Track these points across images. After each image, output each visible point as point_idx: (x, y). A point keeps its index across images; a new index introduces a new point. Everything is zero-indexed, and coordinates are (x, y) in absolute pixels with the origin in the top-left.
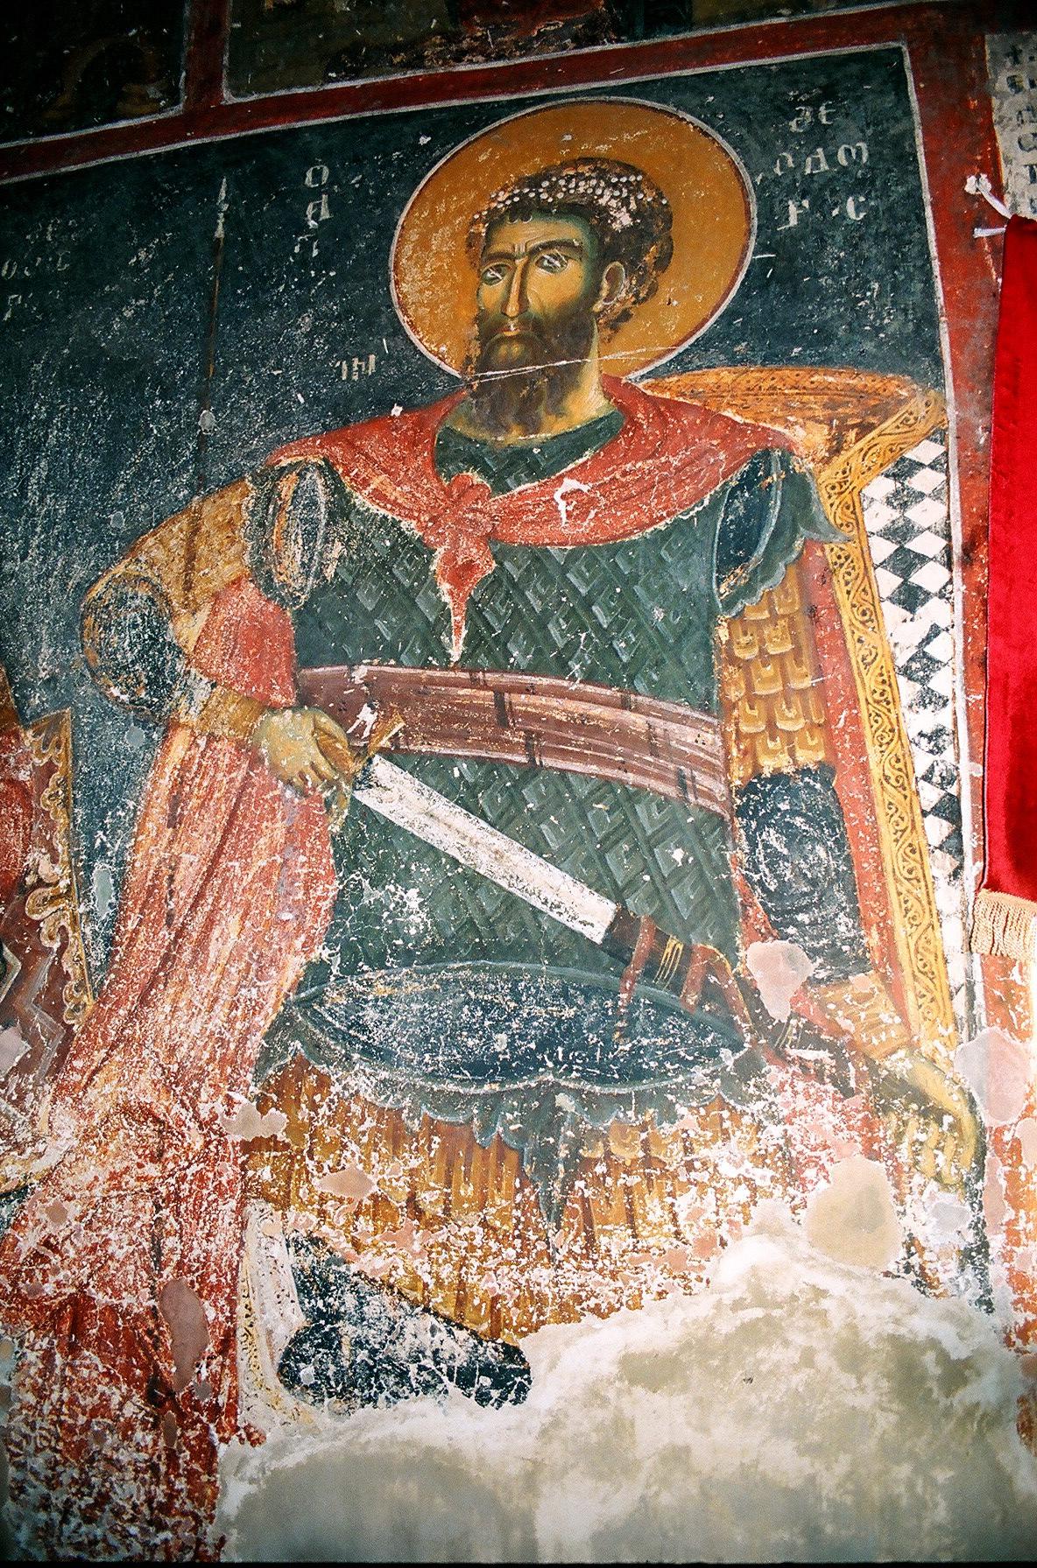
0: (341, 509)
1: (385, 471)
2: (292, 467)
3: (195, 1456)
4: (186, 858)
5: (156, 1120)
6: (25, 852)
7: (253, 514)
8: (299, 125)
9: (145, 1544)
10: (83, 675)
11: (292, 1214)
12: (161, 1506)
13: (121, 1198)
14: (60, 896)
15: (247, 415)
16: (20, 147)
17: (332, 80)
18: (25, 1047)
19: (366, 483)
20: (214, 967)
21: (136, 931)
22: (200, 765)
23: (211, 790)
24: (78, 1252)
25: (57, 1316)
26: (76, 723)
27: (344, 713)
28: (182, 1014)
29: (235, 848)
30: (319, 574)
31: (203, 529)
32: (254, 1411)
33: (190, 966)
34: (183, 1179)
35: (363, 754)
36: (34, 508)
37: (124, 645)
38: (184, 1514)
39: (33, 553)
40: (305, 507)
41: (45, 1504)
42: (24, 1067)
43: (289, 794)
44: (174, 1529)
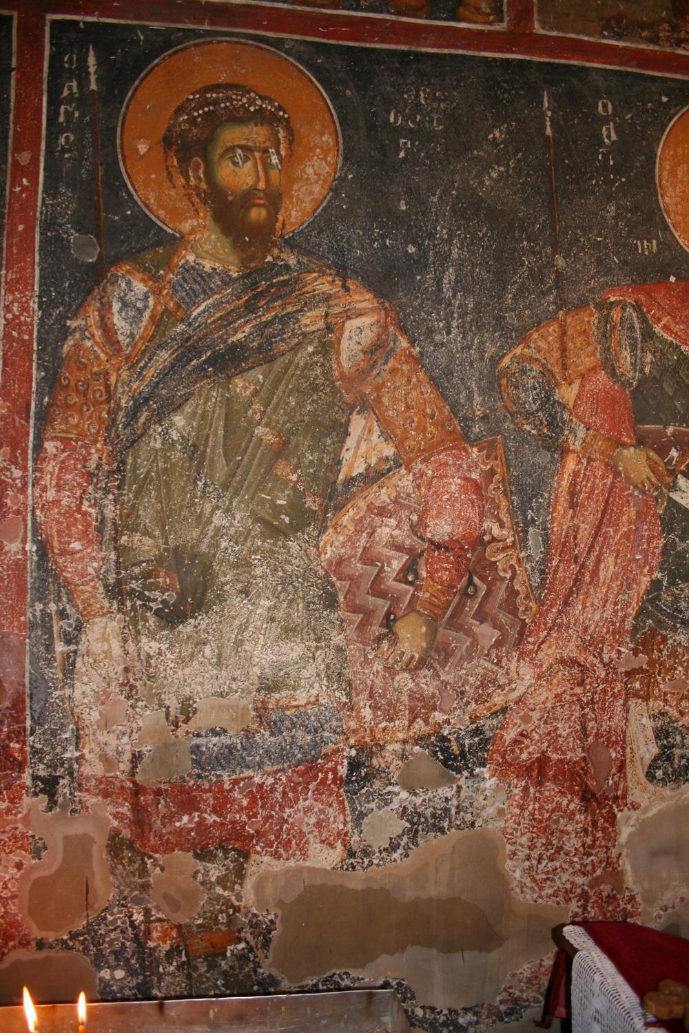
0: (648, 334)
1: (669, 314)
2: (617, 303)
3: (606, 821)
4: (583, 526)
5: (579, 665)
6: (481, 521)
7: (598, 328)
8: (588, 64)
9: (581, 864)
10: (505, 416)
11: (651, 703)
12: (589, 847)
13: (562, 706)
14: (508, 547)
15: (585, 264)
16: (386, 21)
17: (605, 37)
18: (497, 633)
19: (659, 320)
20: (604, 583)
21: (558, 566)
22: (585, 474)
23: (593, 489)
24: (540, 736)
25: (529, 769)
26: (505, 445)
27: (663, 451)
28: (589, 610)
29: (609, 520)
30: (642, 371)
31: (569, 333)
32: (635, 795)
33: (590, 584)
34: (595, 693)
35: (673, 473)
36: (450, 301)
37: (530, 400)
38: (601, 847)
39: (455, 331)
40: (628, 329)
41: (528, 858)
42: (498, 644)
43: (636, 493)
44: (596, 855)
